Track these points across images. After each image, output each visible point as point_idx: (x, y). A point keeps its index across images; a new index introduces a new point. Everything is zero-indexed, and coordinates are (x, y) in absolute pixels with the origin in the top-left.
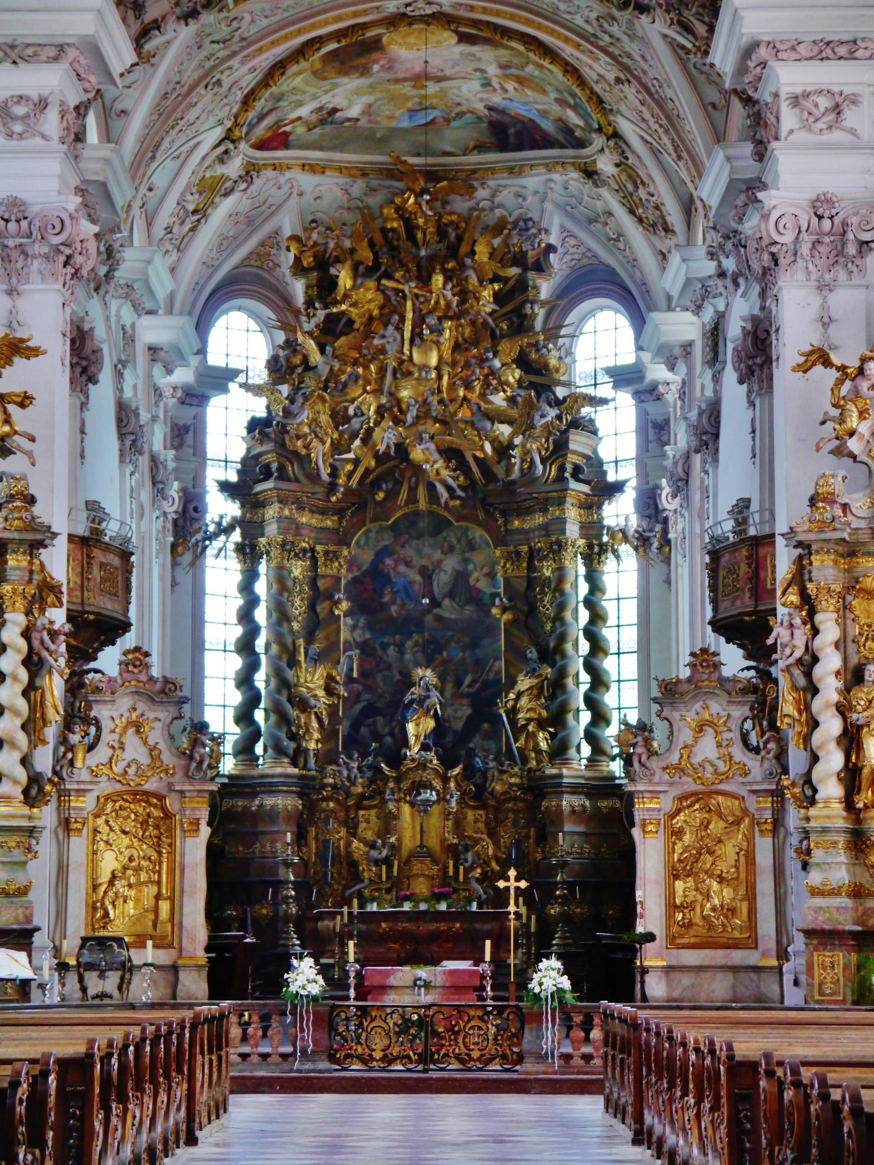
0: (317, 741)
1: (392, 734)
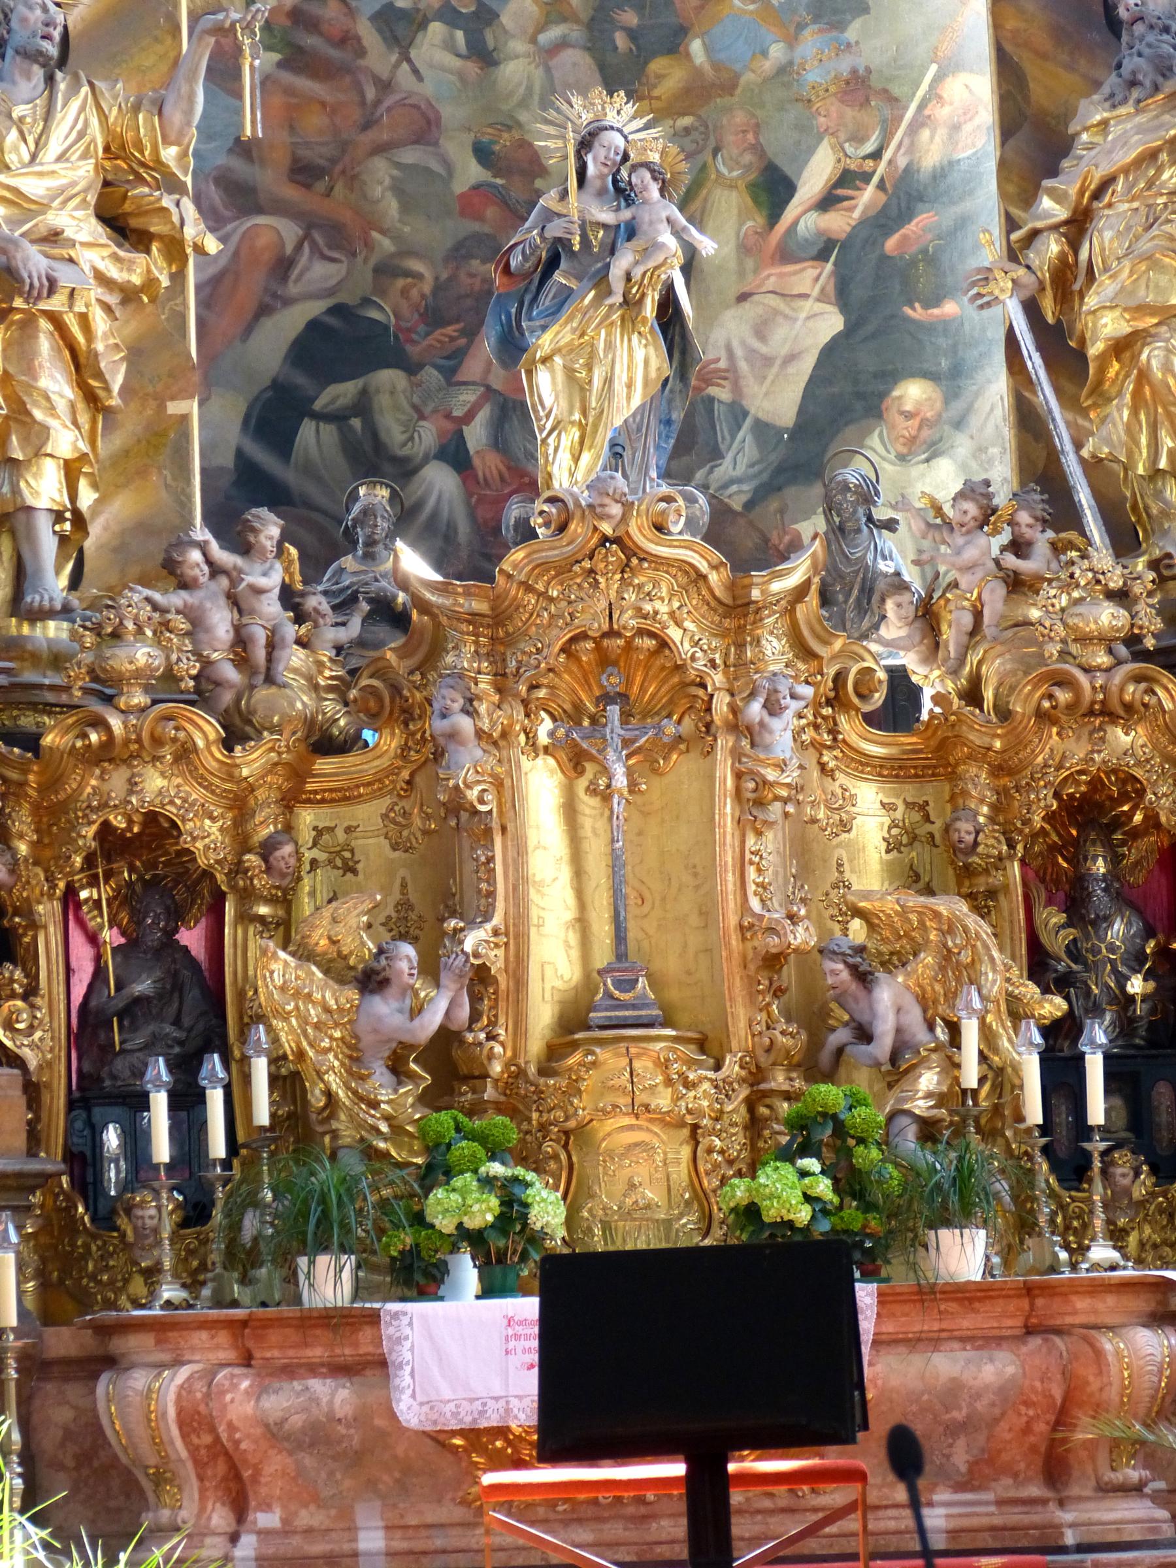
0: (71, 471)
1: (455, 454)
